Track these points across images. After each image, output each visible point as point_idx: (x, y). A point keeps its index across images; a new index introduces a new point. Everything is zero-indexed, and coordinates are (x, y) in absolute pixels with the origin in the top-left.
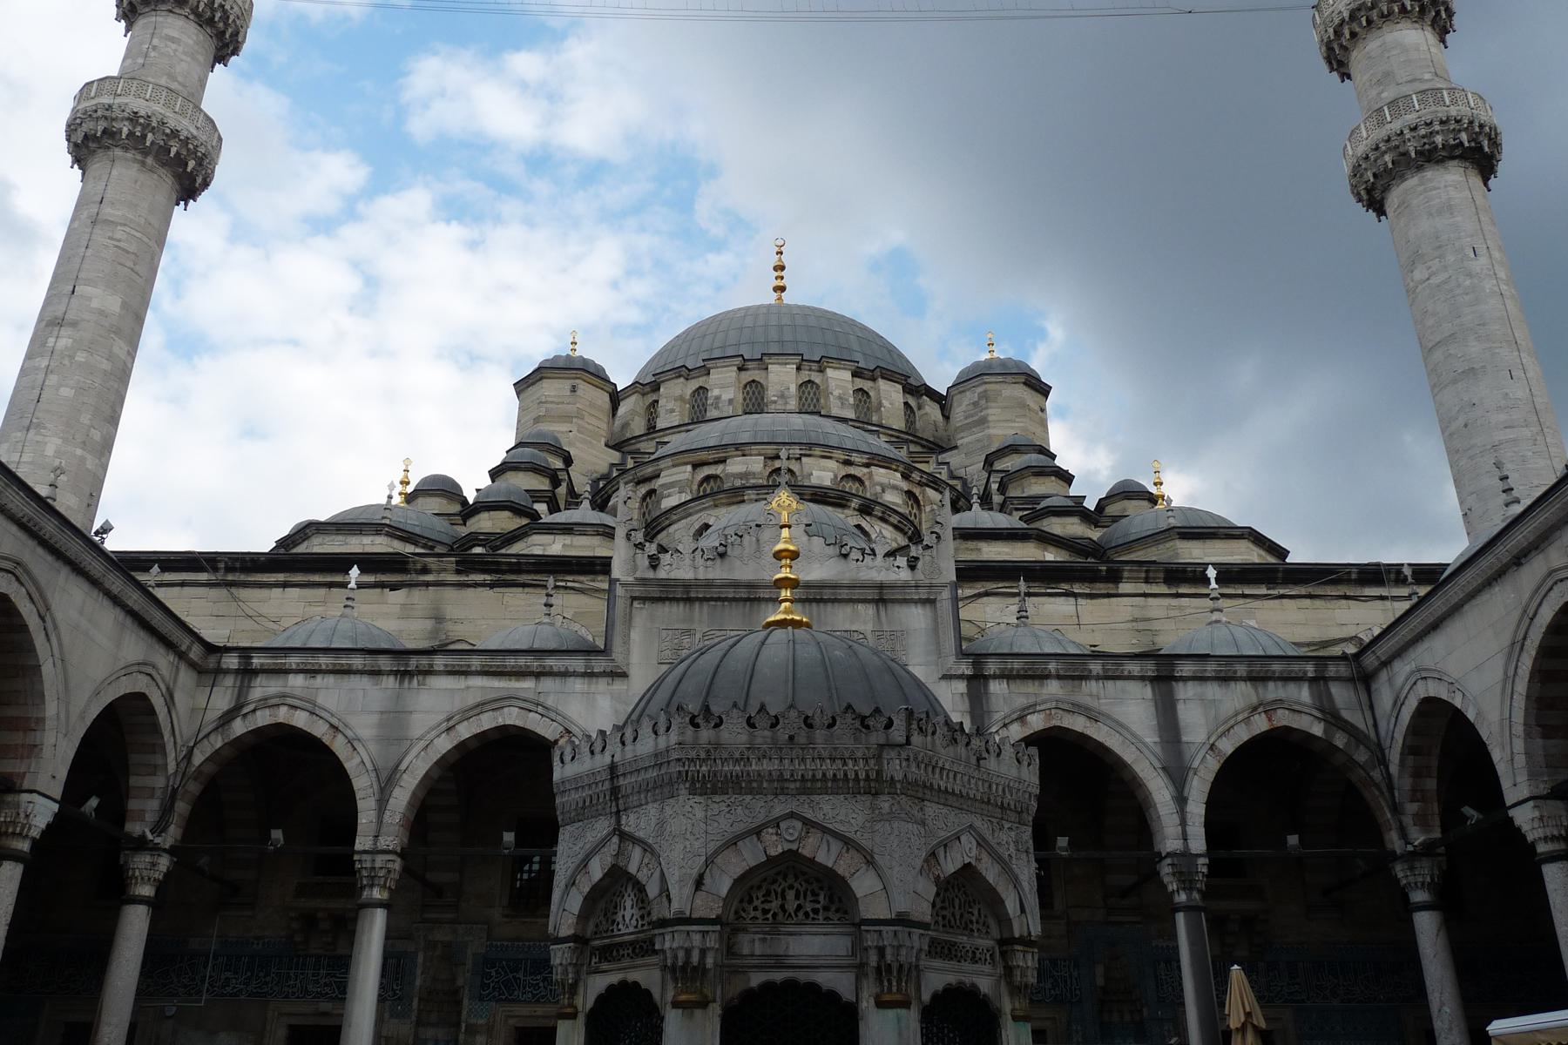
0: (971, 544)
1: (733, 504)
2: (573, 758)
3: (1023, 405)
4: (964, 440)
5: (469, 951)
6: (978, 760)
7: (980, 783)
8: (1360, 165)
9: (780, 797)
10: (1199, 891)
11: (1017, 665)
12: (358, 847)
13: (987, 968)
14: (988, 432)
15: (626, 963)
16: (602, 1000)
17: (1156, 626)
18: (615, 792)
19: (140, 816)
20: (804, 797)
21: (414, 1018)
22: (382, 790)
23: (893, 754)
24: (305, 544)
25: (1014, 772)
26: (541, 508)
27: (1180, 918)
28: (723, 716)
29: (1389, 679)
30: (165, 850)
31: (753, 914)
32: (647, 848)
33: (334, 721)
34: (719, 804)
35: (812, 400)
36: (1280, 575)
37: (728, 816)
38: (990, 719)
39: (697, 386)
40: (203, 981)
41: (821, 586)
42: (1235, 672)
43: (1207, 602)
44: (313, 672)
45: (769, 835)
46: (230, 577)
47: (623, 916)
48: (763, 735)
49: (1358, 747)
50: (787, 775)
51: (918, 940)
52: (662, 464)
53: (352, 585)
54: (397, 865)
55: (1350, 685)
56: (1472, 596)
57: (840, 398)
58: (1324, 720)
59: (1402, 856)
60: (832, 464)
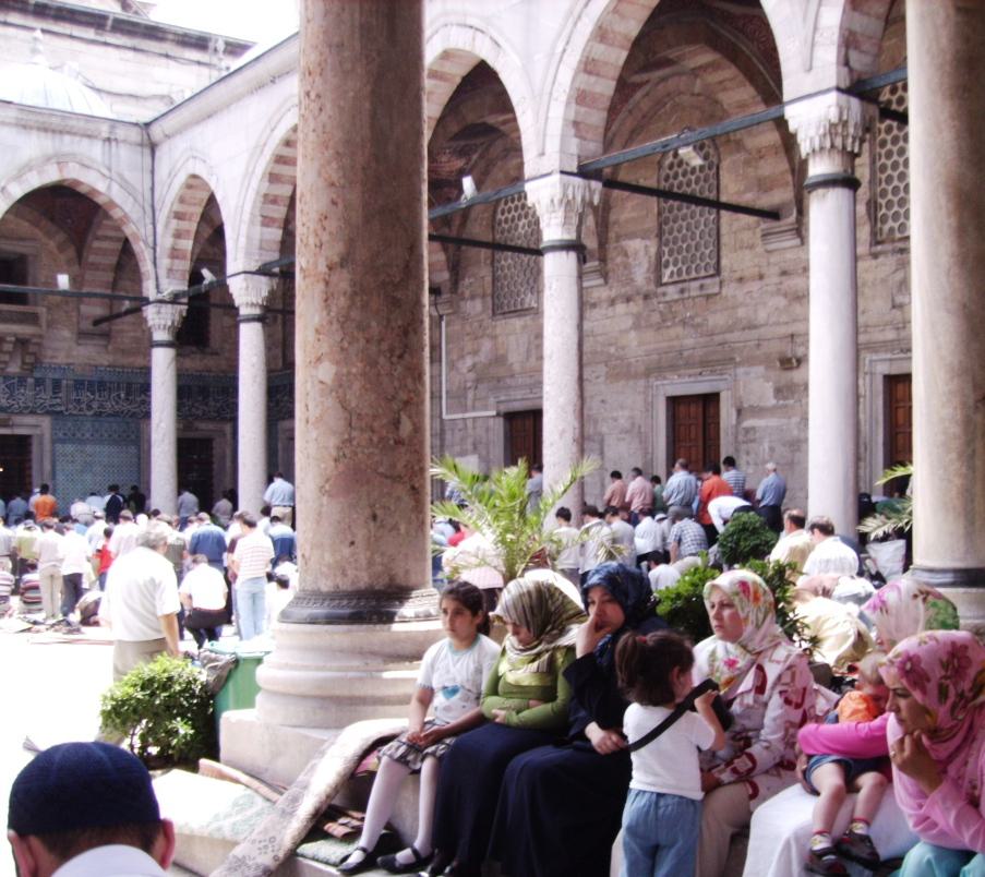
36: (110, 23)
55: (139, 149)
56: (238, 98)
59: (153, 302)
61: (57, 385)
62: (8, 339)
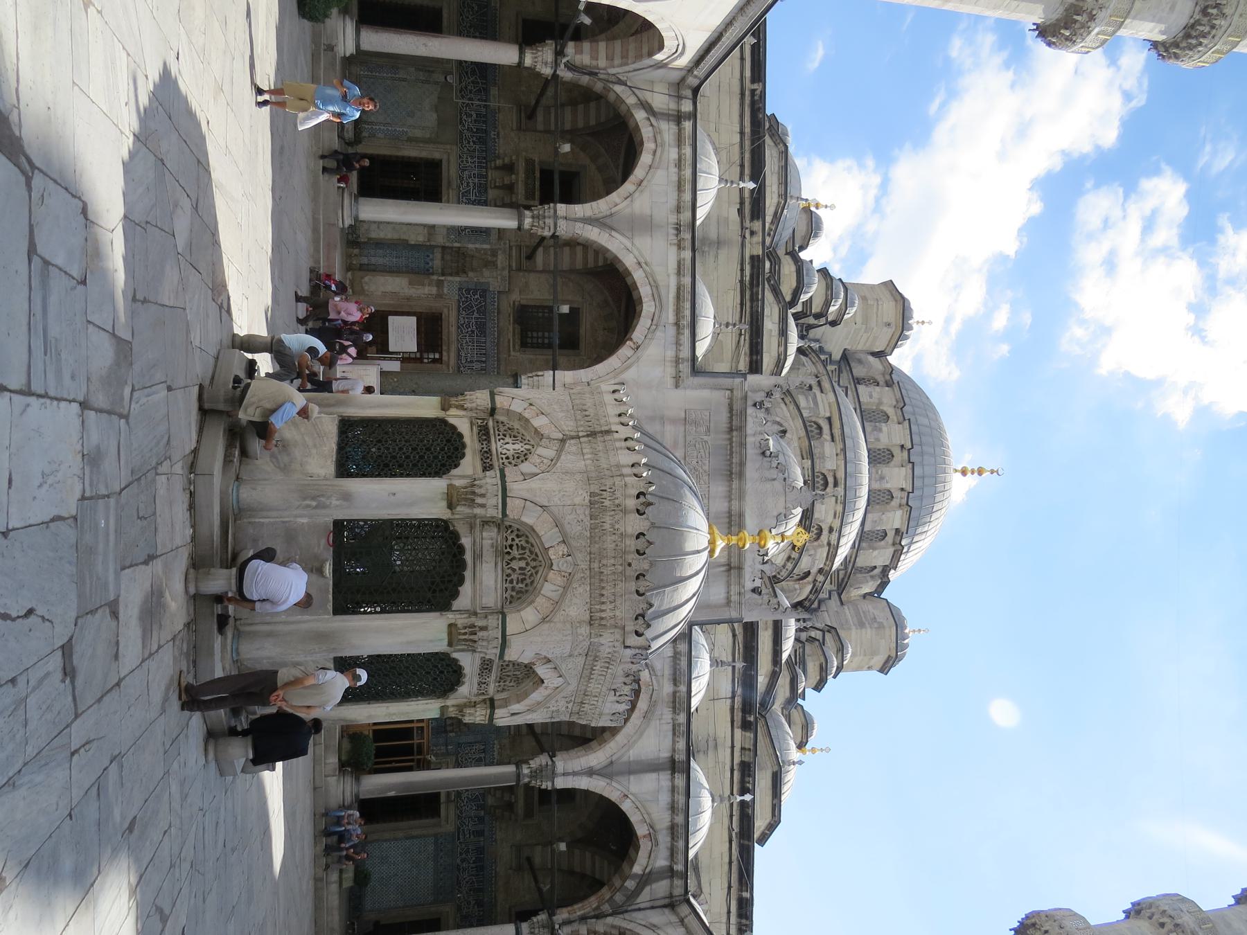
1: (801, 452)
2: (616, 400)
3: (874, 653)
4: (848, 612)
6: (615, 690)
7: (598, 690)
8: (1055, 921)
9: (588, 556)
10: (530, 782)
11: (683, 663)
12: (559, 206)
13: (475, 691)
14: (854, 627)
15: (478, 446)
16: (454, 428)
17: (711, 753)
18: (593, 434)
19: (579, 51)
21: (447, 245)
22: (597, 220)
23: (618, 636)
24: (773, 144)
26: (798, 308)
27: (511, 769)
28: (645, 516)
29: (671, 923)
30: (555, 71)
31: (510, 538)
32: (554, 461)
33: (644, 183)
34: (583, 514)
35: (879, 499)
36: (746, 842)
37: (576, 521)
39: (889, 415)
40: (470, 99)
42: (677, 815)
43: (727, 792)
44: (679, 164)
45: (563, 549)
46: (747, 93)
47: (508, 443)
48: (632, 544)
49: (624, 895)
50: (604, 562)
51: (492, 653)
52: (831, 396)
53: (742, 185)
54: (547, 233)
55: (667, 894)
57: (881, 520)
58: (643, 875)
59: (551, 919)
60: (830, 519)
62: (513, 797)
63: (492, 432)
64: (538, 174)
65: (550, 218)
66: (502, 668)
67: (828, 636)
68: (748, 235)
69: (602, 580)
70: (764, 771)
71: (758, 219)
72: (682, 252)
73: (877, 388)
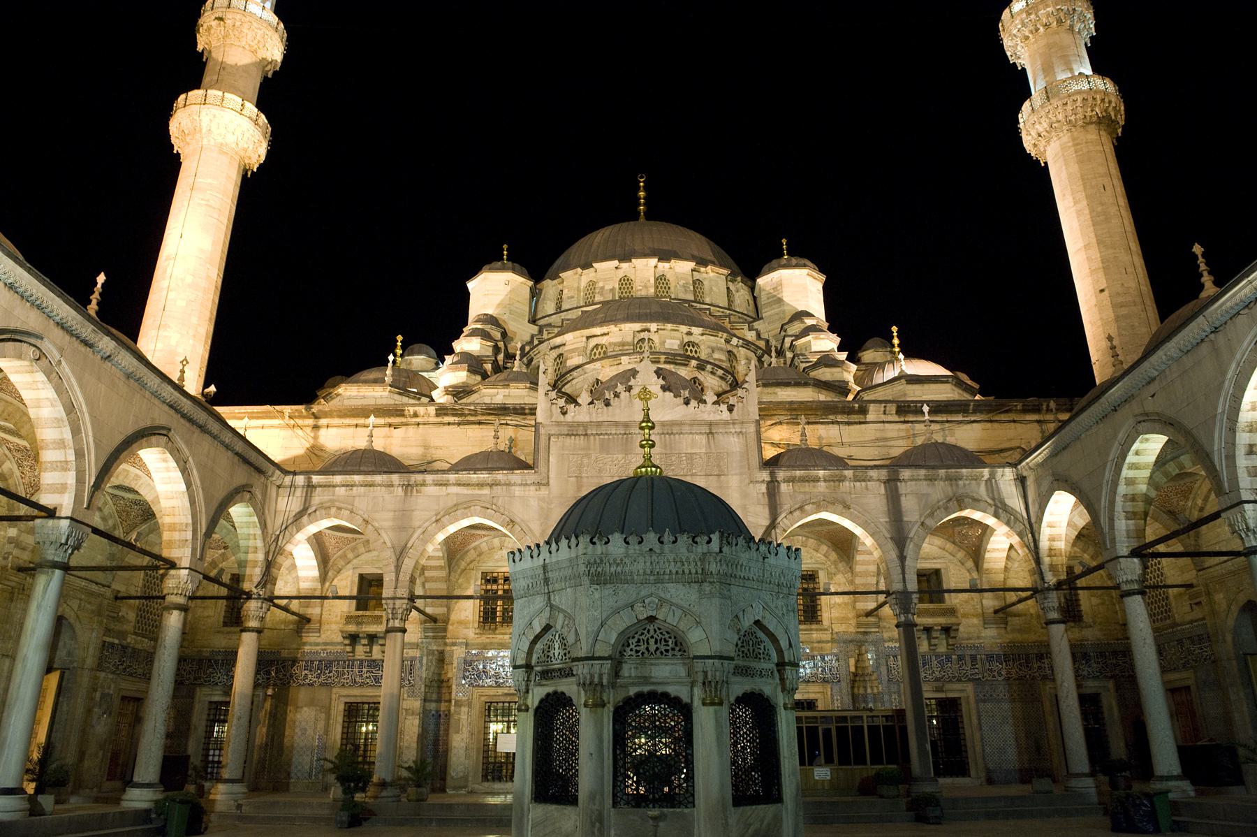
0: (770, 390)
2: (520, 560)
5: (455, 657)
6: (764, 558)
13: (770, 680)
15: (557, 680)
16: (542, 701)
18: (546, 580)
20: (659, 585)
25: (786, 564)
31: (630, 653)
32: (568, 616)
33: (366, 517)
34: (608, 590)
36: (971, 407)
38: (781, 508)
41: (673, 423)
45: (638, 607)
58: (995, 505)
61: (974, 658)
62: (936, 628)
63: (545, 668)
64: (360, 613)
65: (394, 604)
66: (746, 656)
67: (790, 332)
68: (418, 420)
69: (664, 574)
70: (907, 392)
71: (403, 410)
72: (427, 482)
73: (565, 292)
